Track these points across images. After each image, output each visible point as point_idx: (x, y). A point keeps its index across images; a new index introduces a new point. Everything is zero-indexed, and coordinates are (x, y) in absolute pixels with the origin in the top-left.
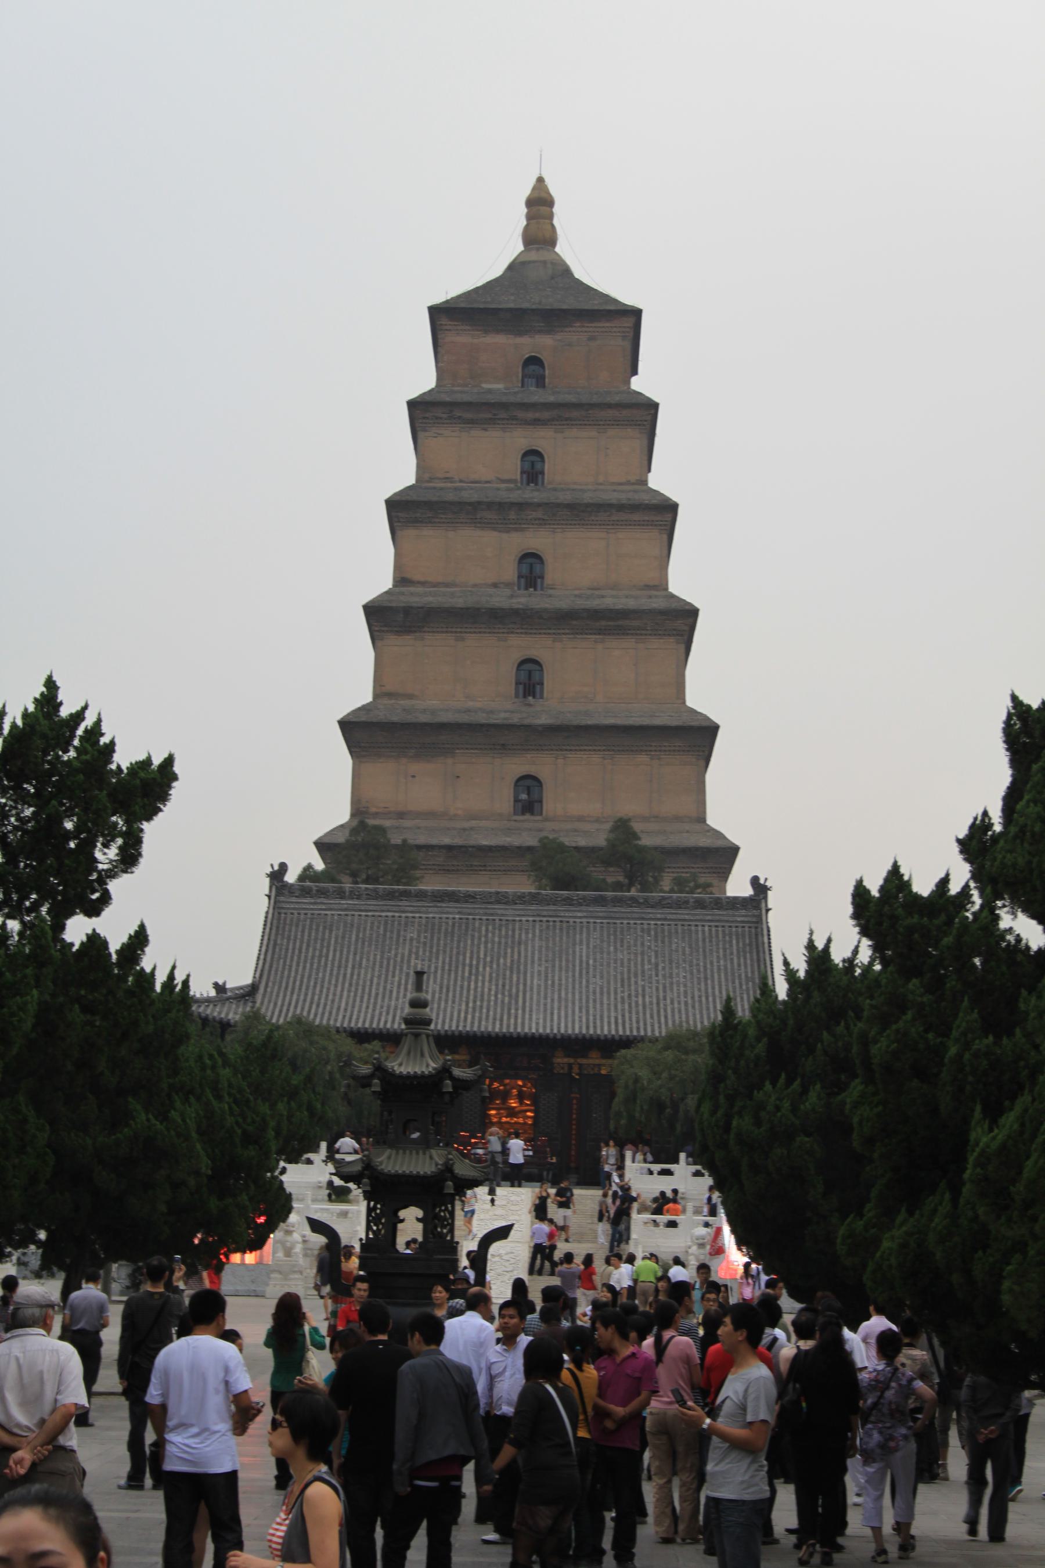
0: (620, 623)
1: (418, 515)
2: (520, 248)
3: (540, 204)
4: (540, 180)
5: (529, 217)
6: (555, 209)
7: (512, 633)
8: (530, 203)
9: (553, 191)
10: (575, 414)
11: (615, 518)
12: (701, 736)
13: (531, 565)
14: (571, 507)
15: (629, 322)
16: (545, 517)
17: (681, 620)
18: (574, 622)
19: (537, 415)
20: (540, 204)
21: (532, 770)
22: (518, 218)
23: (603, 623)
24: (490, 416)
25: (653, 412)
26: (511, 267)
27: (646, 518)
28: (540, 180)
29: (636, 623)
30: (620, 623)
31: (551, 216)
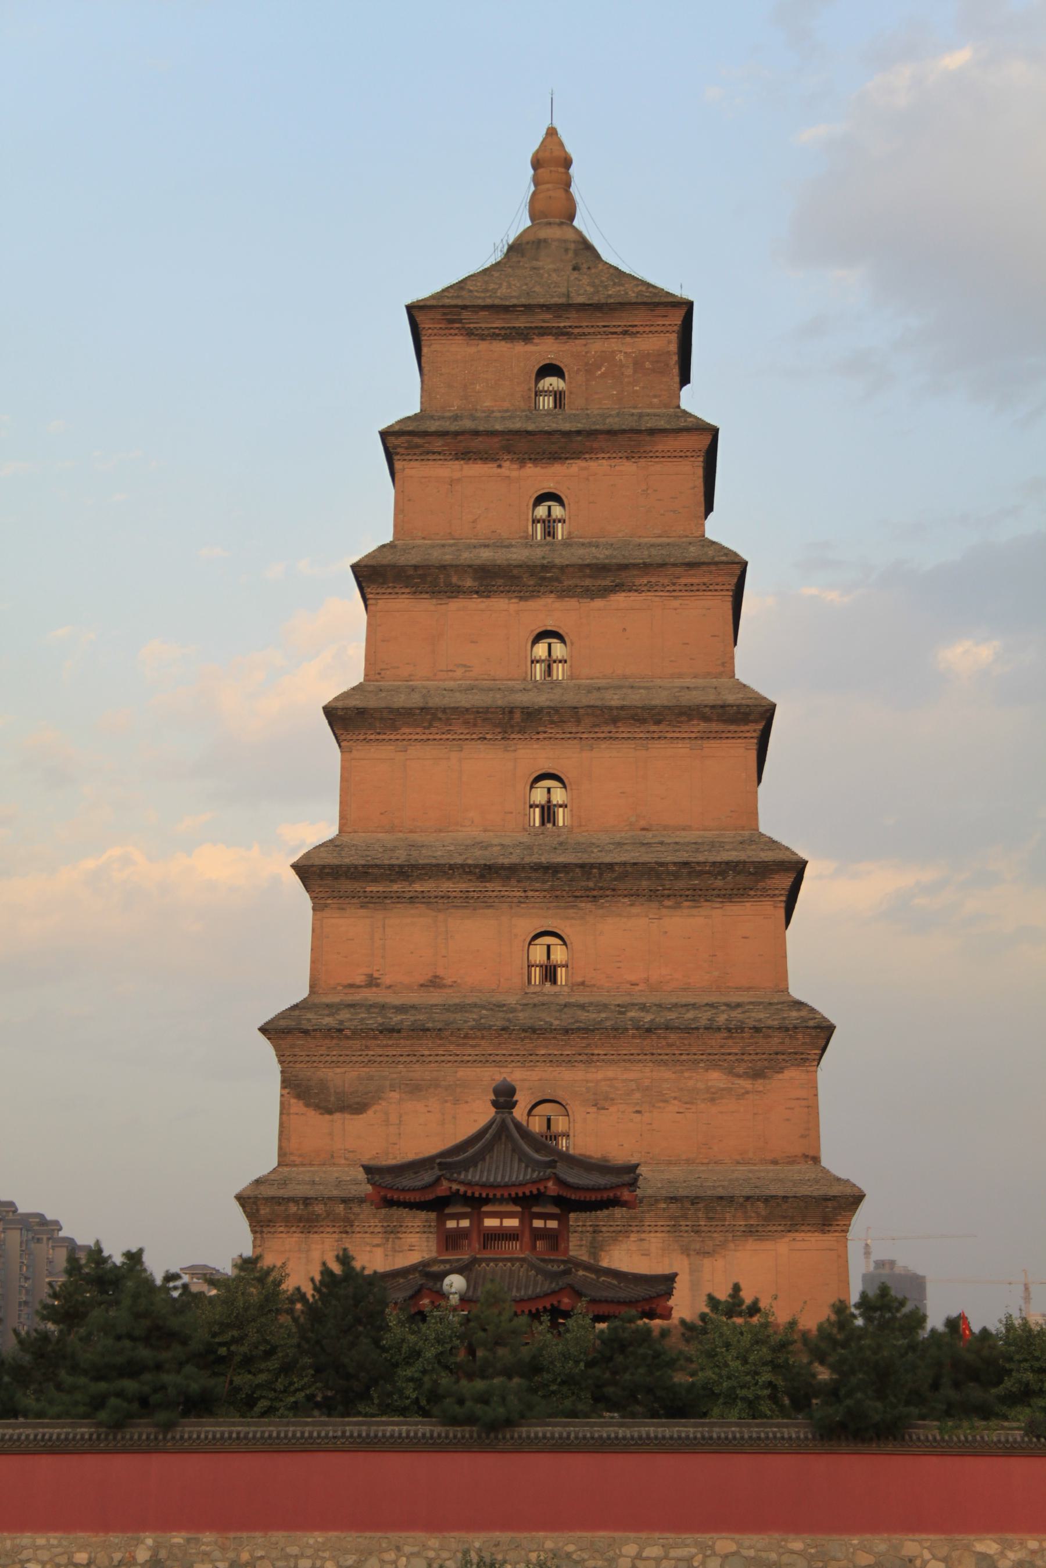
2: (529, 223)
3: (552, 164)
4: (552, 132)
5: (536, 181)
6: (572, 171)
8: (537, 163)
9: (570, 149)
12: (779, 877)
13: (550, 645)
14: (600, 569)
17: (756, 719)
20: (552, 164)
22: (521, 184)
26: (515, 249)
28: (552, 132)
31: (567, 183)
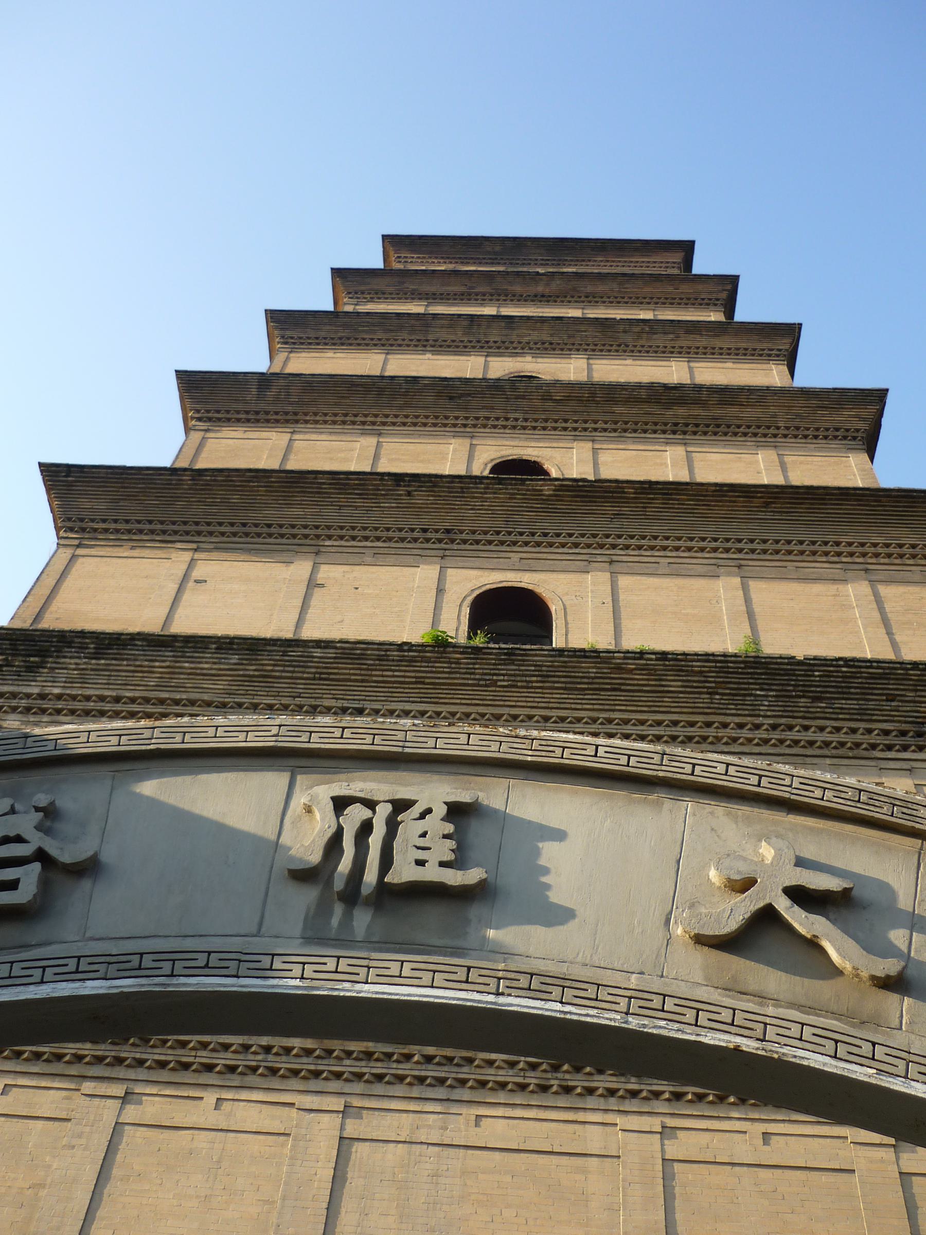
0: (718, 412)
1: (323, 334)
7: (485, 426)
10: (601, 288)
11: (685, 343)
15: (678, 257)
16: (556, 340)
18: (618, 409)
19: (540, 289)
21: (525, 580)
23: (681, 411)
24: (463, 289)
25: (729, 287)
27: (744, 345)
29: (749, 414)
30: (718, 412)
